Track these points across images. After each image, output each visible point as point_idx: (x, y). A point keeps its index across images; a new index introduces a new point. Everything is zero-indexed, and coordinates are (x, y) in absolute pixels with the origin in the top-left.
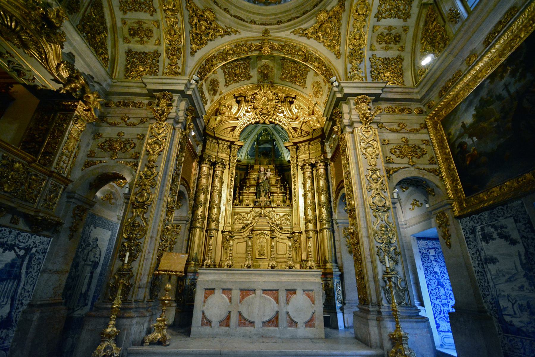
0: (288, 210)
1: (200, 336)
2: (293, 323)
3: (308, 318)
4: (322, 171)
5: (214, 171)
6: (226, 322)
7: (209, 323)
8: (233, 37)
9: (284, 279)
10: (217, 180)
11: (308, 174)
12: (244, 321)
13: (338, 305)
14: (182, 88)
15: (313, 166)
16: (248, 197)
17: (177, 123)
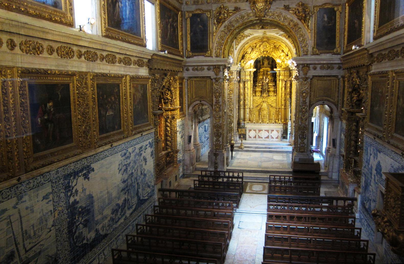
0: (275, 98)
1: (248, 140)
2: (272, 138)
3: (277, 136)
4: (289, 85)
5: (244, 85)
6: (255, 137)
7: (251, 138)
8: (251, 37)
9: (271, 126)
10: (246, 89)
11: (283, 85)
12: (259, 137)
13: (289, 133)
14: (236, 69)
15: (286, 81)
16: (258, 89)
17: (235, 81)
